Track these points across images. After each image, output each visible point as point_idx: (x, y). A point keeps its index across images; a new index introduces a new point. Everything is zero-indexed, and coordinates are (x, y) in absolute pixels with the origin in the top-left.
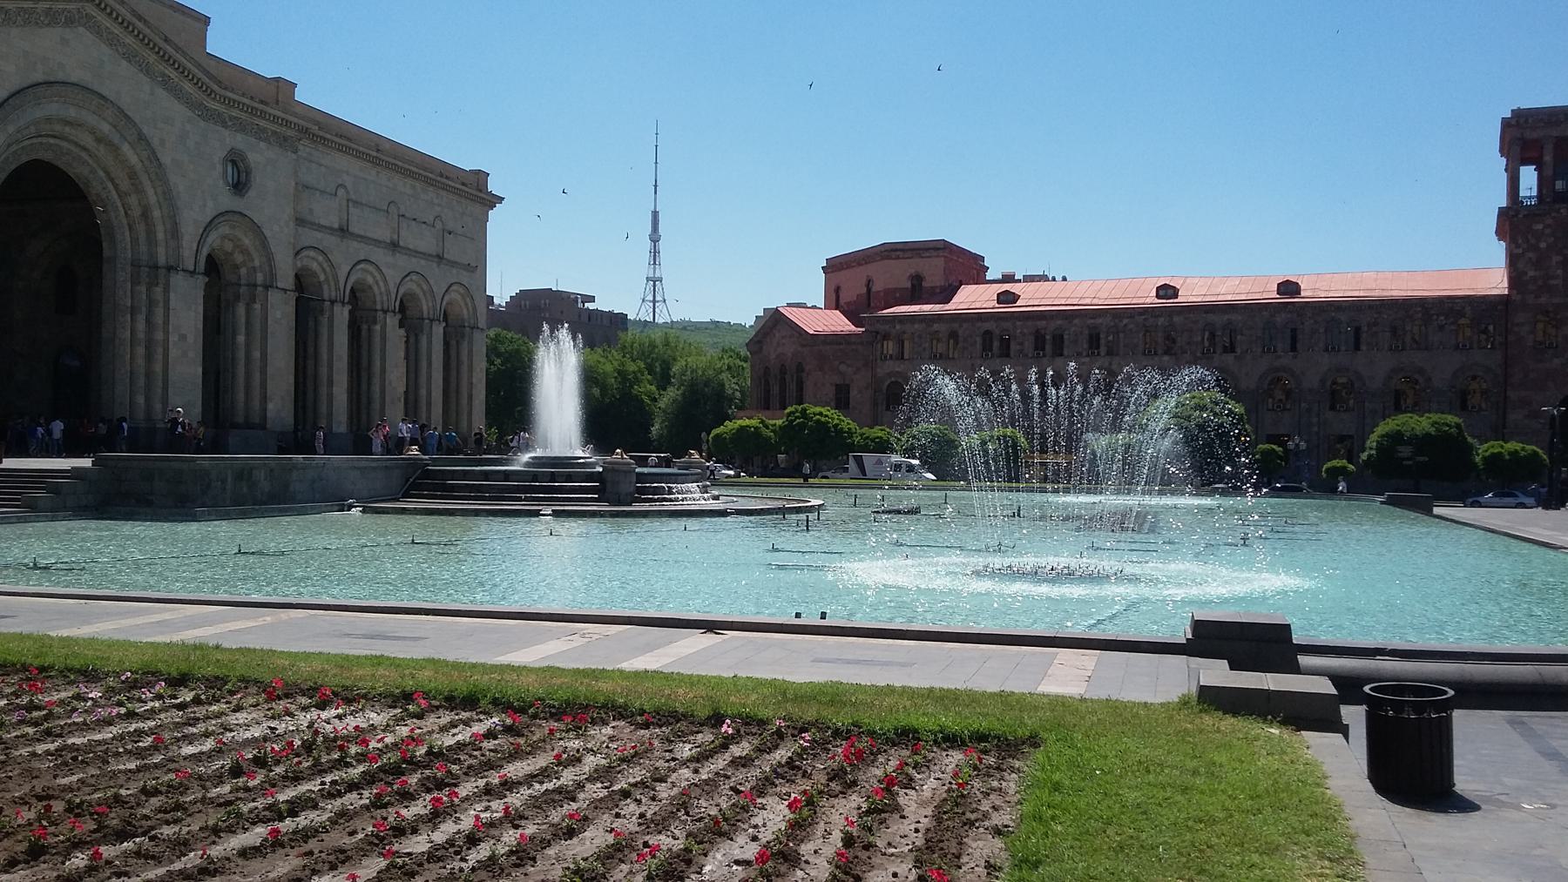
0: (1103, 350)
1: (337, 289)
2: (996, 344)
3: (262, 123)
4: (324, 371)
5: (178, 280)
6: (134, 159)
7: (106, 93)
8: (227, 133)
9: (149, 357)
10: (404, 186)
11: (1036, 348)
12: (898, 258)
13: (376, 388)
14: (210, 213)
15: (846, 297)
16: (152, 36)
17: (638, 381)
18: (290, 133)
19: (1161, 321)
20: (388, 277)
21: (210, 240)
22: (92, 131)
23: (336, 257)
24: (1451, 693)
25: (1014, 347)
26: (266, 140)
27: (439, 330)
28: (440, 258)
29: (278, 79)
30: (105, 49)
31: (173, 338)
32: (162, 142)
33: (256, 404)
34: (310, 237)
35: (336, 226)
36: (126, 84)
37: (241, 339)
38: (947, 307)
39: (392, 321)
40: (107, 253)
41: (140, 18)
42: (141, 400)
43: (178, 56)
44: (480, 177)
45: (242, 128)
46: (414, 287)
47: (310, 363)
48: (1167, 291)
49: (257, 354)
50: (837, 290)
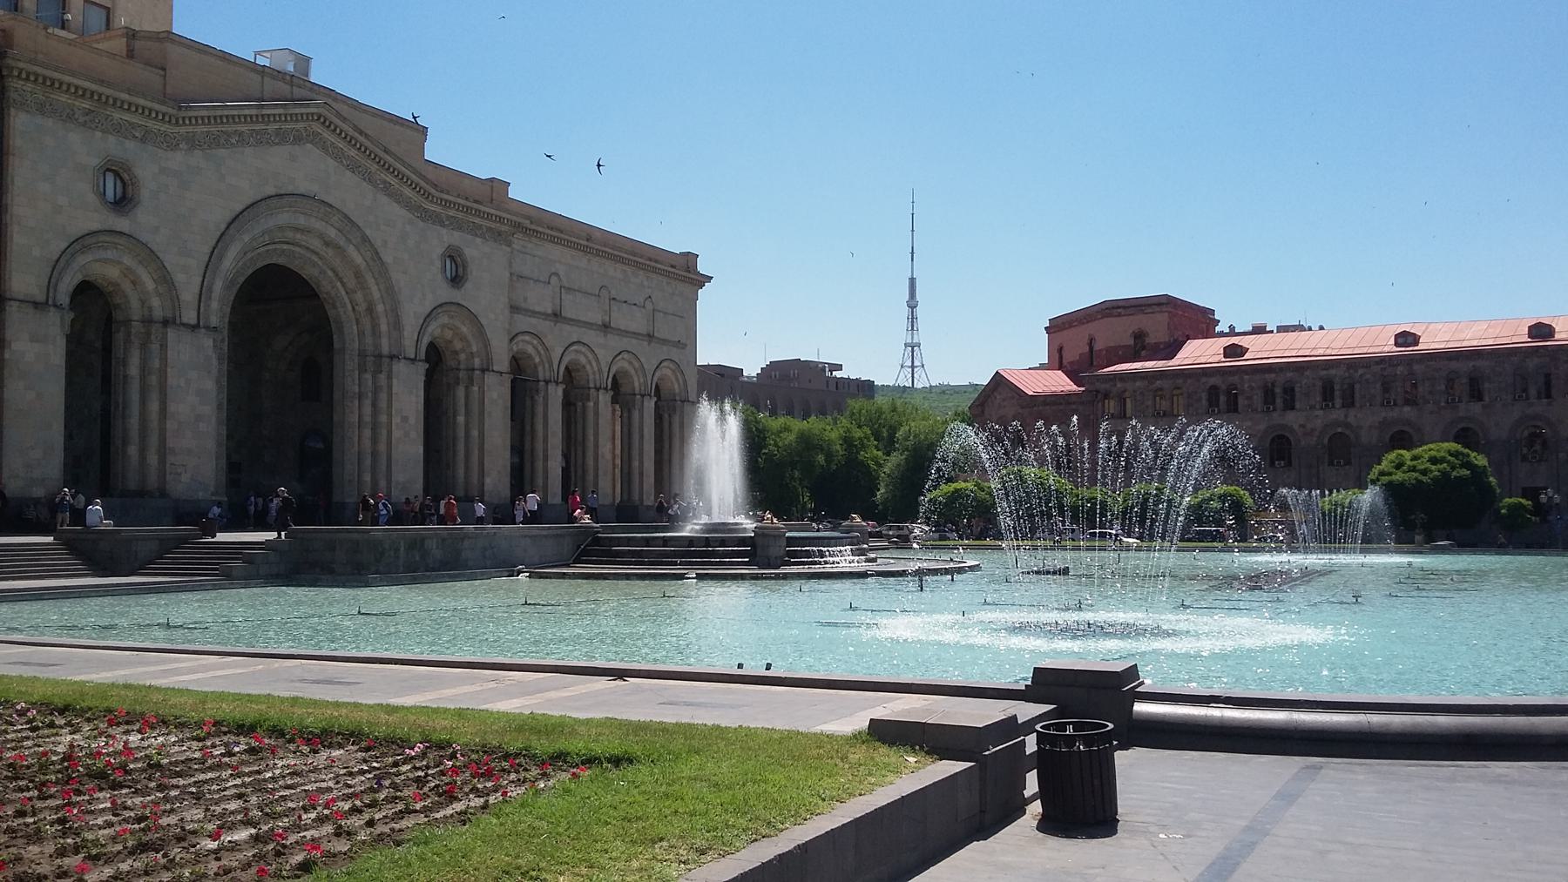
0: (1338, 402)
1: (551, 365)
2: (1223, 399)
3: (478, 220)
4: (539, 446)
5: (400, 368)
6: (359, 260)
8: (444, 231)
9: (375, 440)
10: (614, 271)
11: (1266, 402)
12: (1119, 315)
13: (590, 462)
15: (1069, 357)
17: (863, 447)
19: (1400, 370)
20: (601, 357)
21: (430, 329)
22: (321, 236)
23: (549, 340)
24: (1111, 726)
25: (1241, 401)
26: (482, 236)
27: (650, 404)
28: (650, 337)
29: (492, 180)
30: (331, 161)
31: (396, 420)
33: (475, 479)
34: (523, 323)
36: (349, 192)
37: (461, 419)
38: (1171, 363)
39: (604, 398)
40: (336, 345)
41: (361, 133)
42: (367, 478)
44: (690, 259)
45: (458, 226)
46: (626, 365)
47: (528, 439)
48: (1406, 338)
49: (475, 433)
50: (1060, 350)
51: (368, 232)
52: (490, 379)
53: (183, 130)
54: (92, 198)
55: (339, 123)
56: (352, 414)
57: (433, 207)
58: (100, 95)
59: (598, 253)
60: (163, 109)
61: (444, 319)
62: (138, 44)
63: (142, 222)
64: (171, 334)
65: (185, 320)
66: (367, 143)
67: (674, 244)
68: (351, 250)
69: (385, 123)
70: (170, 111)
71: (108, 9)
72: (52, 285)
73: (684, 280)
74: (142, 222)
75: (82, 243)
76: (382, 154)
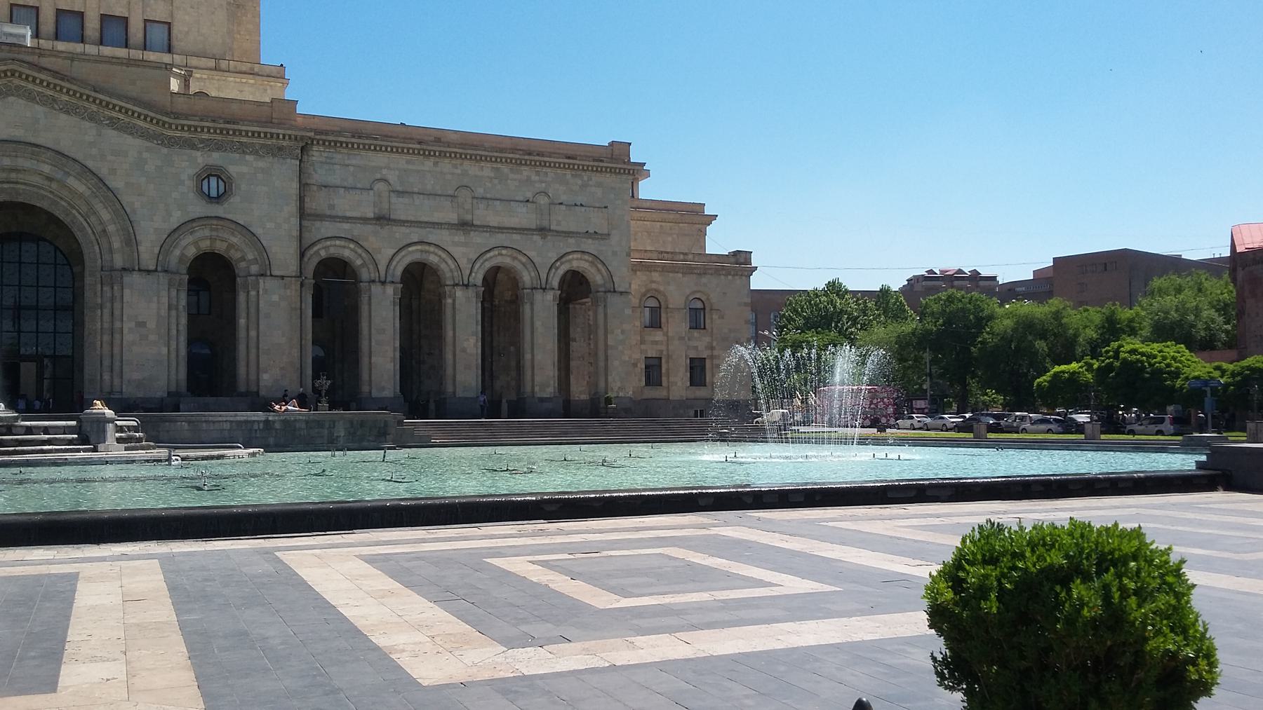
3: (244, 140)
6: (81, 188)
7: (40, 141)
8: (199, 154)
10: (487, 170)
13: (449, 356)
14: (176, 218)
16: (82, 91)
22: (41, 174)
23: (372, 242)
26: (255, 153)
28: (543, 231)
30: (40, 110)
31: (127, 326)
32: (113, 171)
33: (253, 377)
34: (327, 229)
35: (371, 215)
36: (65, 131)
37: (242, 322)
41: (62, 79)
42: (106, 377)
43: (115, 101)
45: (219, 147)
46: (508, 261)
49: (253, 333)
51: (90, 164)
52: (264, 284)
56: (95, 323)
59: (443, 155)
61: (207, 233)
67: (600, 137)
68: (71, 181)
73: (599, 170)
76: (93, 94)
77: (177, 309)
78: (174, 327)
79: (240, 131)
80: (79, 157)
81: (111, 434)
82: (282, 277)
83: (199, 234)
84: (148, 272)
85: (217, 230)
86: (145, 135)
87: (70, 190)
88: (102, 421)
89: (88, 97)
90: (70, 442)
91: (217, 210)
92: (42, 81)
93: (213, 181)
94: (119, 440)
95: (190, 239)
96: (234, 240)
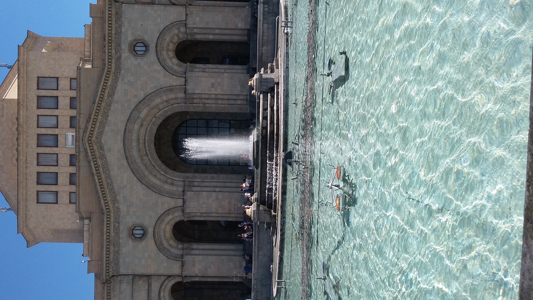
3: (114, 32)
7: (123, 129)
8: (123, 55)
16: (95, 109)
18: (114, 12)
26: (120, 26)
29: (91, 16)
30: (107, 129)
31: (213, 91)
32: (136, 96)
33: (240, 32)
36: (117, 118)
37: (211, 37)
41: (90, 118)
42: (239, 102)
45: (119, 45)
49: (217, 31)
51: (132, 107)
52: (190, 24)
53: (111, 206)
54: (143, 243)
55: (89, 130)
56: (212, 107)
57: (113, 65)
58: (107, 245)
60: (105, 220)
61: (164, 52)
62: (84, 216)
63: (149, 222)
64: (187, 210)
65: (181, 205)
66: (94, 112)
68: (142, 115)
69: (82, 93)
70: (105, 217)
71: (71, 79)
72: (176, 258)
74: (149, 222)
75: (160, 247)
76: (96, 104)
77: (205, 68)
78: (213, 70)
79: (109, 33)
80: (129, 112)
81: (269, 75)
82: (187, 15)
83: (165, 56)
84: (186, 81)
85: (163, 48)
86: (116, 80)
87: (147, 116)
88: (261, 80)
89: (98, 106)
90: (273, 97)
91: (152, 47)
92: (92, 127)
93: (137, 49)
94: (272, 71)
95: (168, 61)
96: (168, 39)
